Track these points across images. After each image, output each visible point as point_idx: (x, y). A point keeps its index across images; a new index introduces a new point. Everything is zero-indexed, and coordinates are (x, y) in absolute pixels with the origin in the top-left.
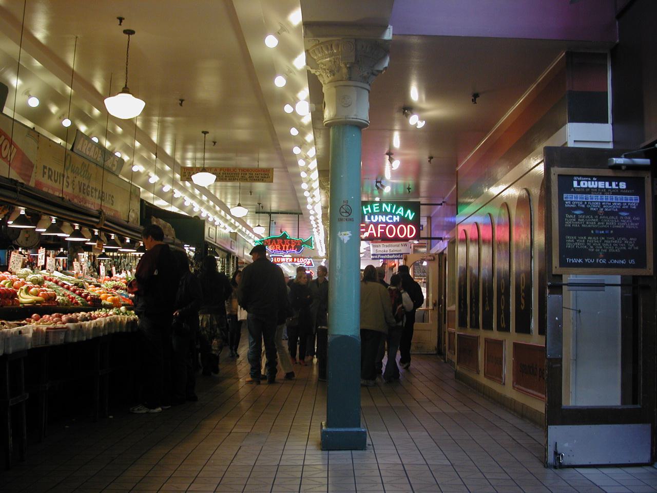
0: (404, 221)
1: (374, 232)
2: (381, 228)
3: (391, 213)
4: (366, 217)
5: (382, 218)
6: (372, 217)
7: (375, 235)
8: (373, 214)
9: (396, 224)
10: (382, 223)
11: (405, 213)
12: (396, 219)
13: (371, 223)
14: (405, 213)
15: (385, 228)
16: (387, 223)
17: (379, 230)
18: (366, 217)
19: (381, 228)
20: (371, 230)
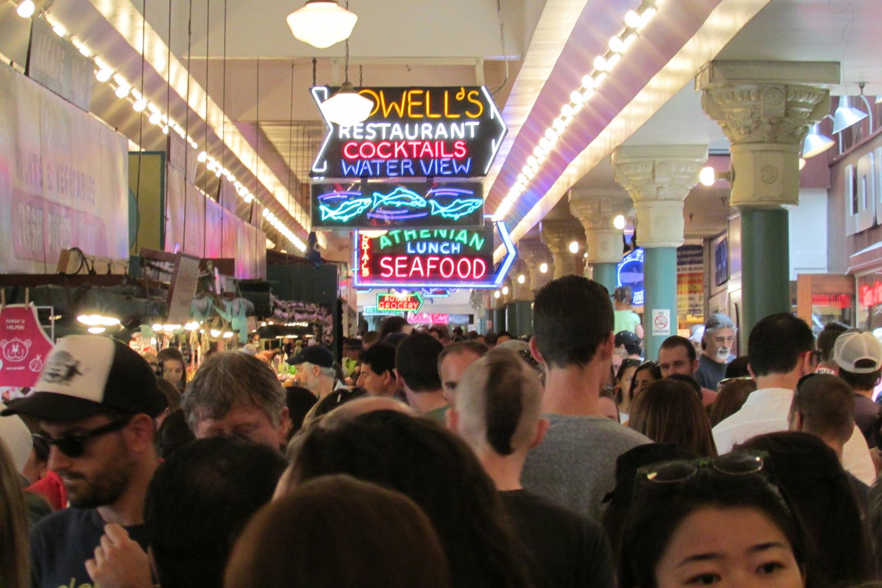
0: (468, 252)
1: (420, 269)
2: (432, 263)
3: (447, 239)
4: (409, 245)
5: (433, 248)
6: (418, 245)
7: (432, 155)
8: (421, 241)
9: (456, 257)
10: (433, 255)
11: (469, 237)
12: (456, 248)
13: (417, 254)
14: (469, 237)
15: (437, 263)
16: (441, 256)
17: (429, 267)
18: (409, 245)
19: (432, 263)
20: (427, 147)
